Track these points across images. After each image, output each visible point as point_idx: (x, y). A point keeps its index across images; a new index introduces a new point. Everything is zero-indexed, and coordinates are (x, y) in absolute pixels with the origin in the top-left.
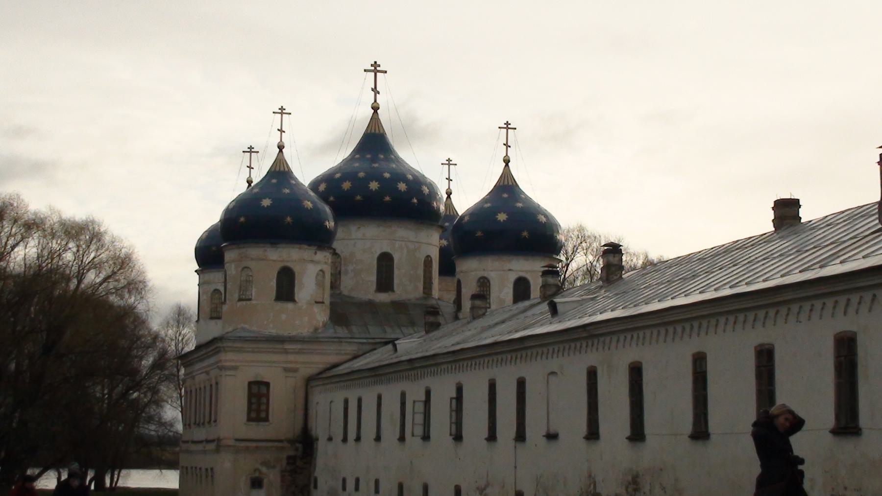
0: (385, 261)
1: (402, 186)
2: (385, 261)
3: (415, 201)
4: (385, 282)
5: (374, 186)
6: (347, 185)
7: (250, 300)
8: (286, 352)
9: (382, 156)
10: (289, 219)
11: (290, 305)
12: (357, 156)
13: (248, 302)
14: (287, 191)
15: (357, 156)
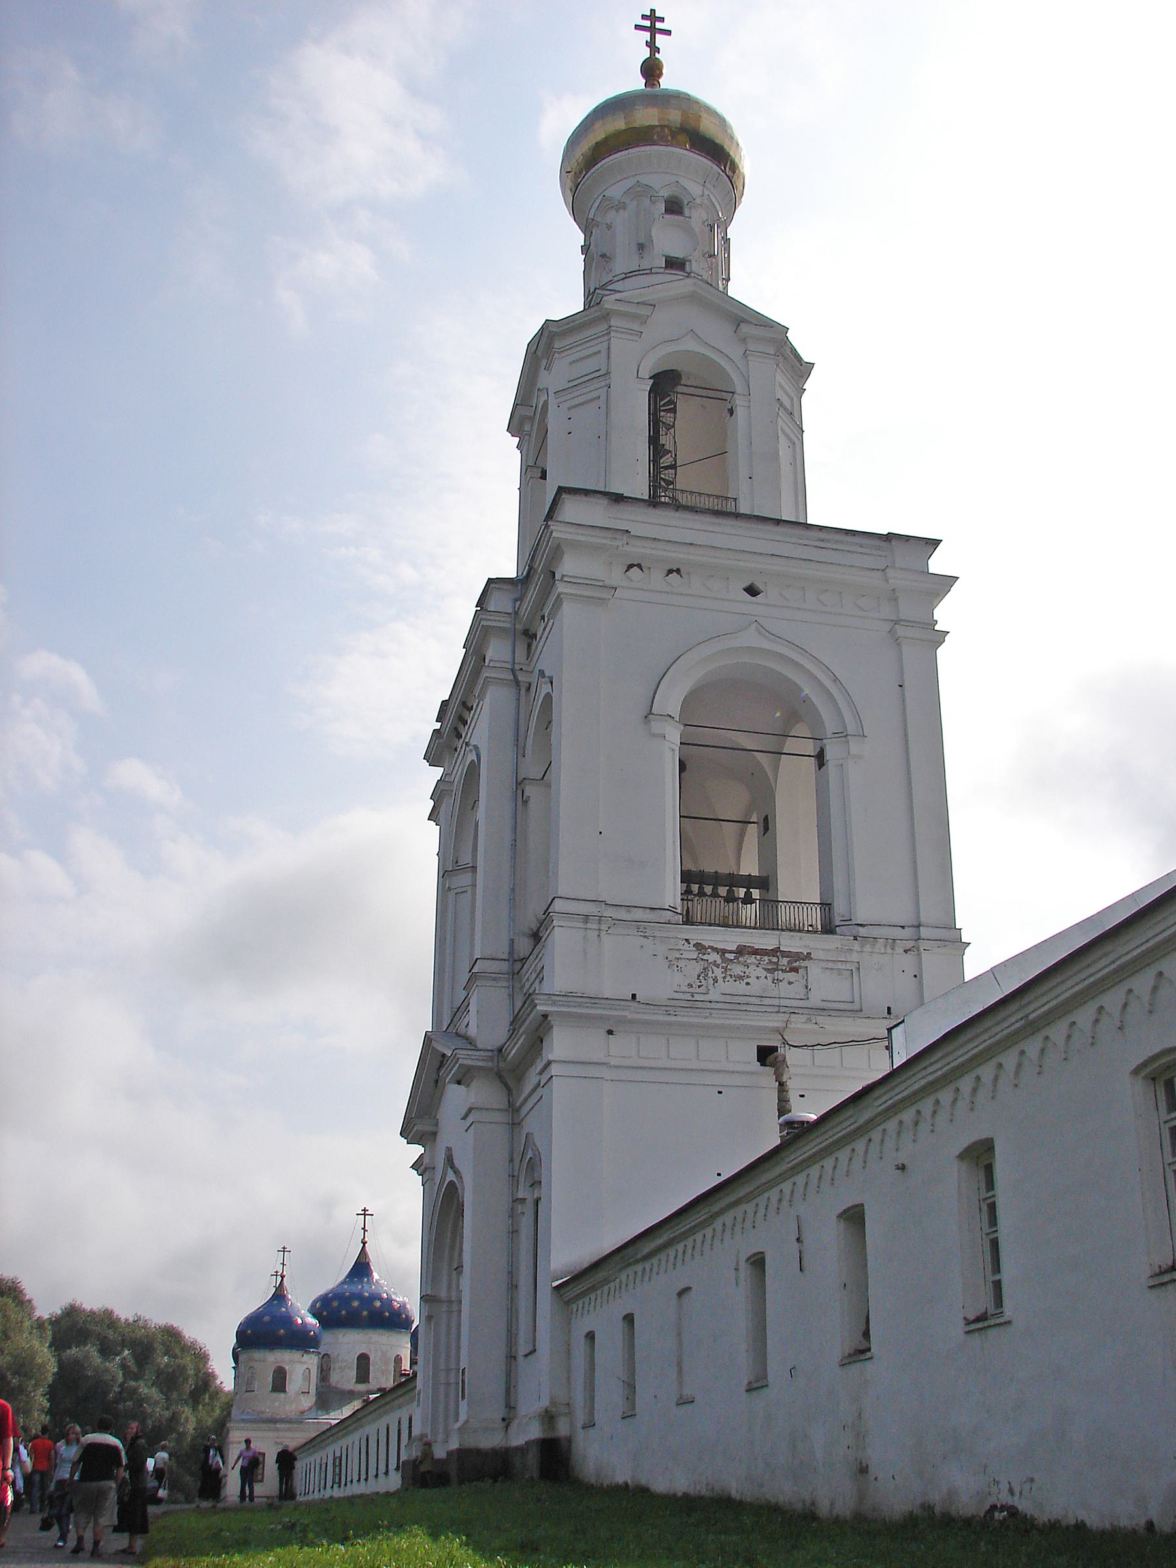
0: (363, 1360)
1: (378, 1304)
2: (363, 1360)
3: (387, 1314)
4: (363, 1374)
5: (356, 1304)
6: (335, 1304)
7: (253, 1391)
8: (277, 1430)
9: (366, 1279)
10: (282, 1331)
11: (282, 1395)
12: (347, 1280)
13: (253, 1393)
14: (284, 1309)
15: (347, 1280)
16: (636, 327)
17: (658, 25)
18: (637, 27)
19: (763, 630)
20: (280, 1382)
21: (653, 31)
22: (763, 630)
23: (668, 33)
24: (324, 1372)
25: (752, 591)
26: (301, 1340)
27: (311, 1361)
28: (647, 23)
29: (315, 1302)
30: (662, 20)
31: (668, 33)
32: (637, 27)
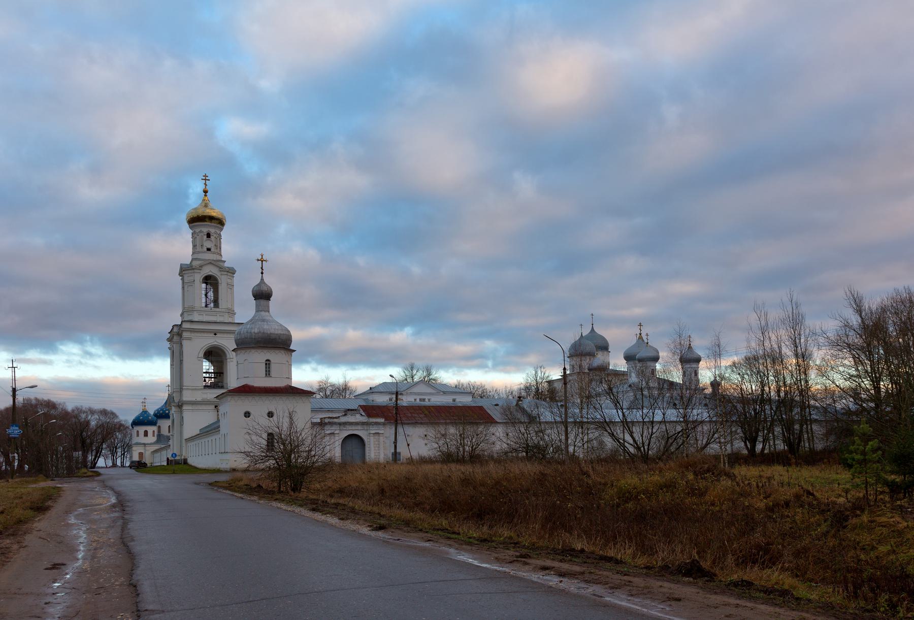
6: (161, 412)
16: (199, 271)
17: (207, 178)
18: (202, 179)
19: (217, 342)
20: (146, 434)
21: (205, 180)
22: (217, 342)
23: (209, 180)
24: (159, 431)
25: (215, 334)
26: (152, 423)
27: (155, 428)
28: (204, 178)
29: (155, 411)
30: (207, 176)
31: (209, 180)
32: (202, 179)
